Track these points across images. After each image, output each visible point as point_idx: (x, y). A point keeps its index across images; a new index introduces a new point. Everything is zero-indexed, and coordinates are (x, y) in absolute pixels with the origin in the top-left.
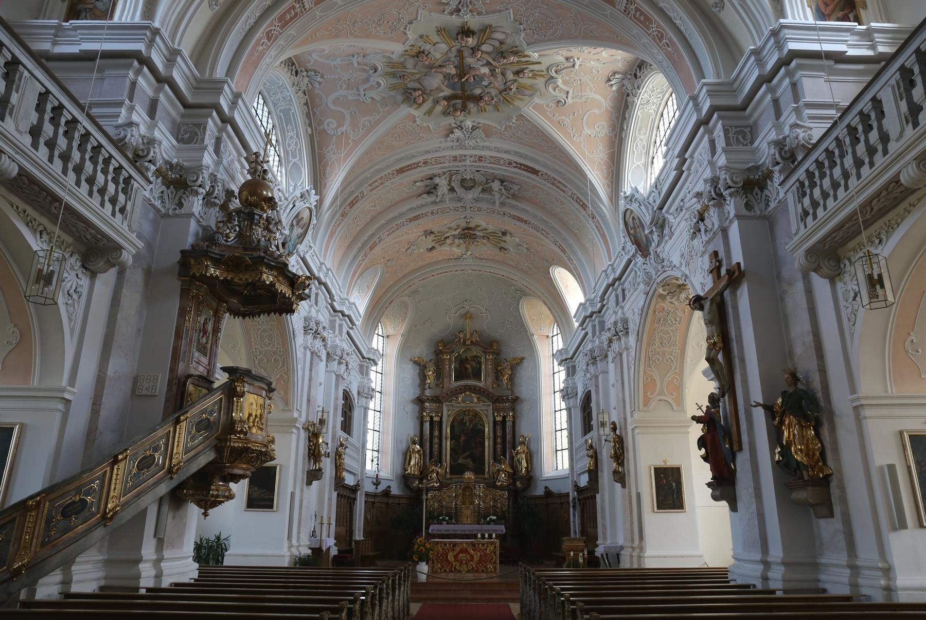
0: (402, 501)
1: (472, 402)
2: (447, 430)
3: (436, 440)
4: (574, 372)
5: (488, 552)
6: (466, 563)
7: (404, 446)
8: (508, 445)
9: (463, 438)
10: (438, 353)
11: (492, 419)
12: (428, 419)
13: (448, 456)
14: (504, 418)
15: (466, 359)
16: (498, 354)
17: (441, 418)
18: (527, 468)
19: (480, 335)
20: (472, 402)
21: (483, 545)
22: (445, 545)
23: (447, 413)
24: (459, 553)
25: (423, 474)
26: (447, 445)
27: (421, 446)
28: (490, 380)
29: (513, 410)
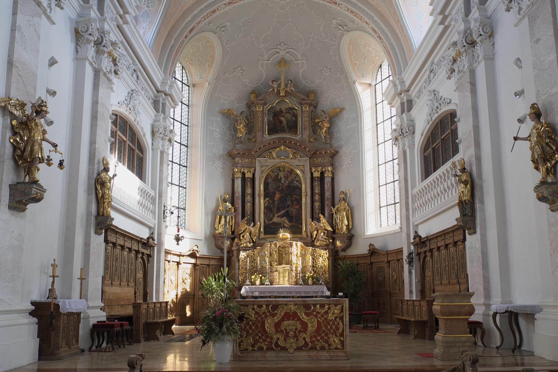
0: (212, 262)
1: (287, 157)
2: (260, 187)
3: (248, 198)
4: (410, 108)
5: (331, 317)
6: (296, 337)
7: (213, 205)
8: (326, 203)
9: (277, 196)
10: (250, 105)
11: (309, 176)
12: (240, 175)
13: (262, 215)
14: (322, 173)
15: (281, 111)
16: (315, 107)
17: (254, 174)
18: (348, 226)
19: (296, 86)
20: (287, 157)
21: (322, 306)
22: (260, 306)
23: (261, 168)
24: (282, 320)
25: (234, 236)
26: (261, 203)
27: (233, 204)
28: (306, 133)
29: (332, 165)
